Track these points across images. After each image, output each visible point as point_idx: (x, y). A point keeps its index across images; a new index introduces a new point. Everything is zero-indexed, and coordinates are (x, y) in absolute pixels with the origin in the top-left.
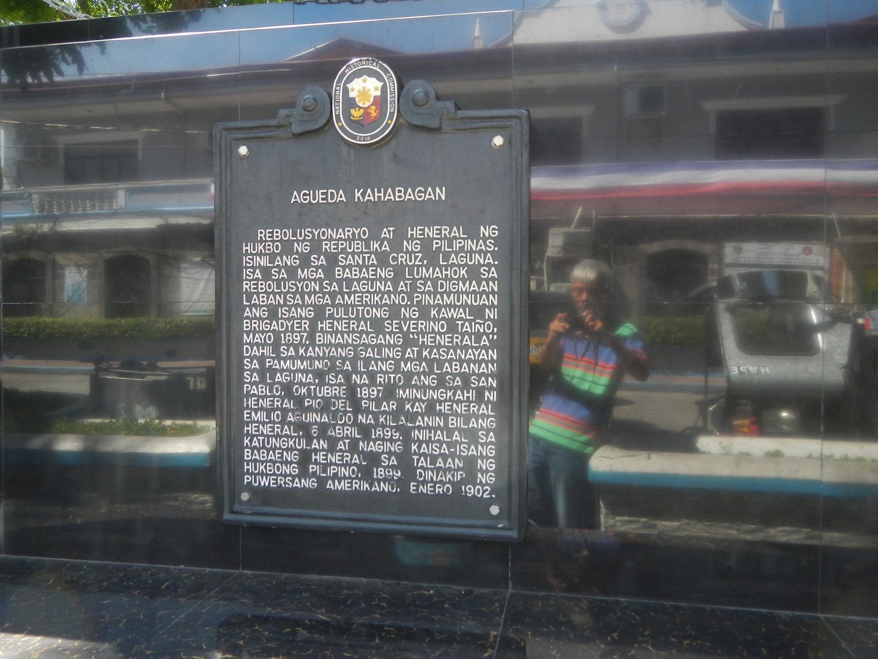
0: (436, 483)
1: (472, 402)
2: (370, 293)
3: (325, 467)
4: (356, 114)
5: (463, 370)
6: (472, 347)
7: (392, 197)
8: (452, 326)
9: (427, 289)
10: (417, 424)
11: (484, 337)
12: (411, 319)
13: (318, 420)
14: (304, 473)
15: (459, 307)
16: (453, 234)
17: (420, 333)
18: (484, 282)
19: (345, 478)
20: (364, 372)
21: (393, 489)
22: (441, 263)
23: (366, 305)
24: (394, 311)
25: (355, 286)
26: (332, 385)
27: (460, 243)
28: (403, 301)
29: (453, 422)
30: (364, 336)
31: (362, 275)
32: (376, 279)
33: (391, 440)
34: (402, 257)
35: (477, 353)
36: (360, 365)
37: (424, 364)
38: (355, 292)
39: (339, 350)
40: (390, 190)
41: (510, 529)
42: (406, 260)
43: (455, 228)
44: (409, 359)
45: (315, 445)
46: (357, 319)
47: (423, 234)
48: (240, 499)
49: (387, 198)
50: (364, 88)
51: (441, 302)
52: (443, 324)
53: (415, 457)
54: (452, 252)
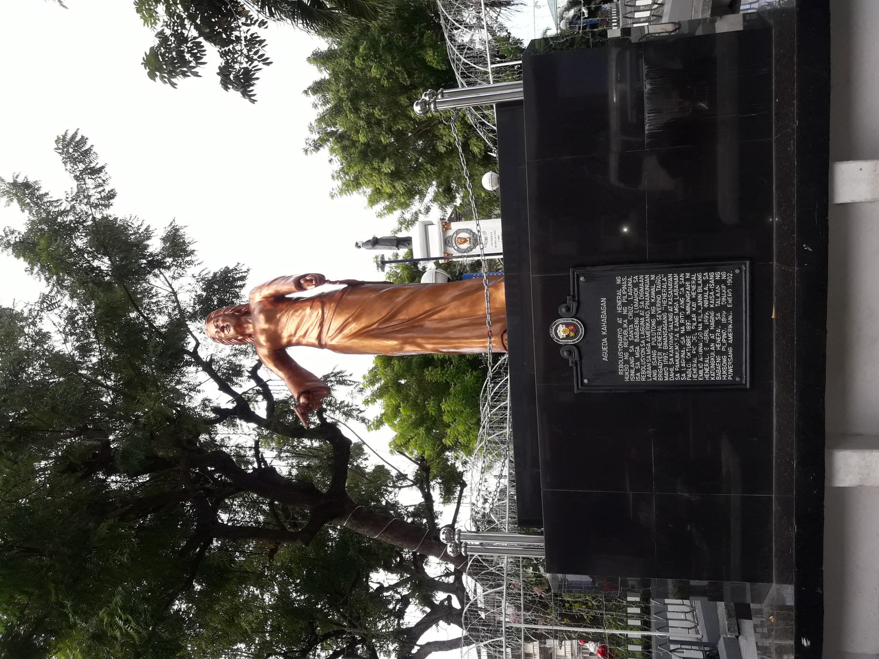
3: (723, 344)
4: (572, 334)
33: (709, 316)
41: (745, 264)
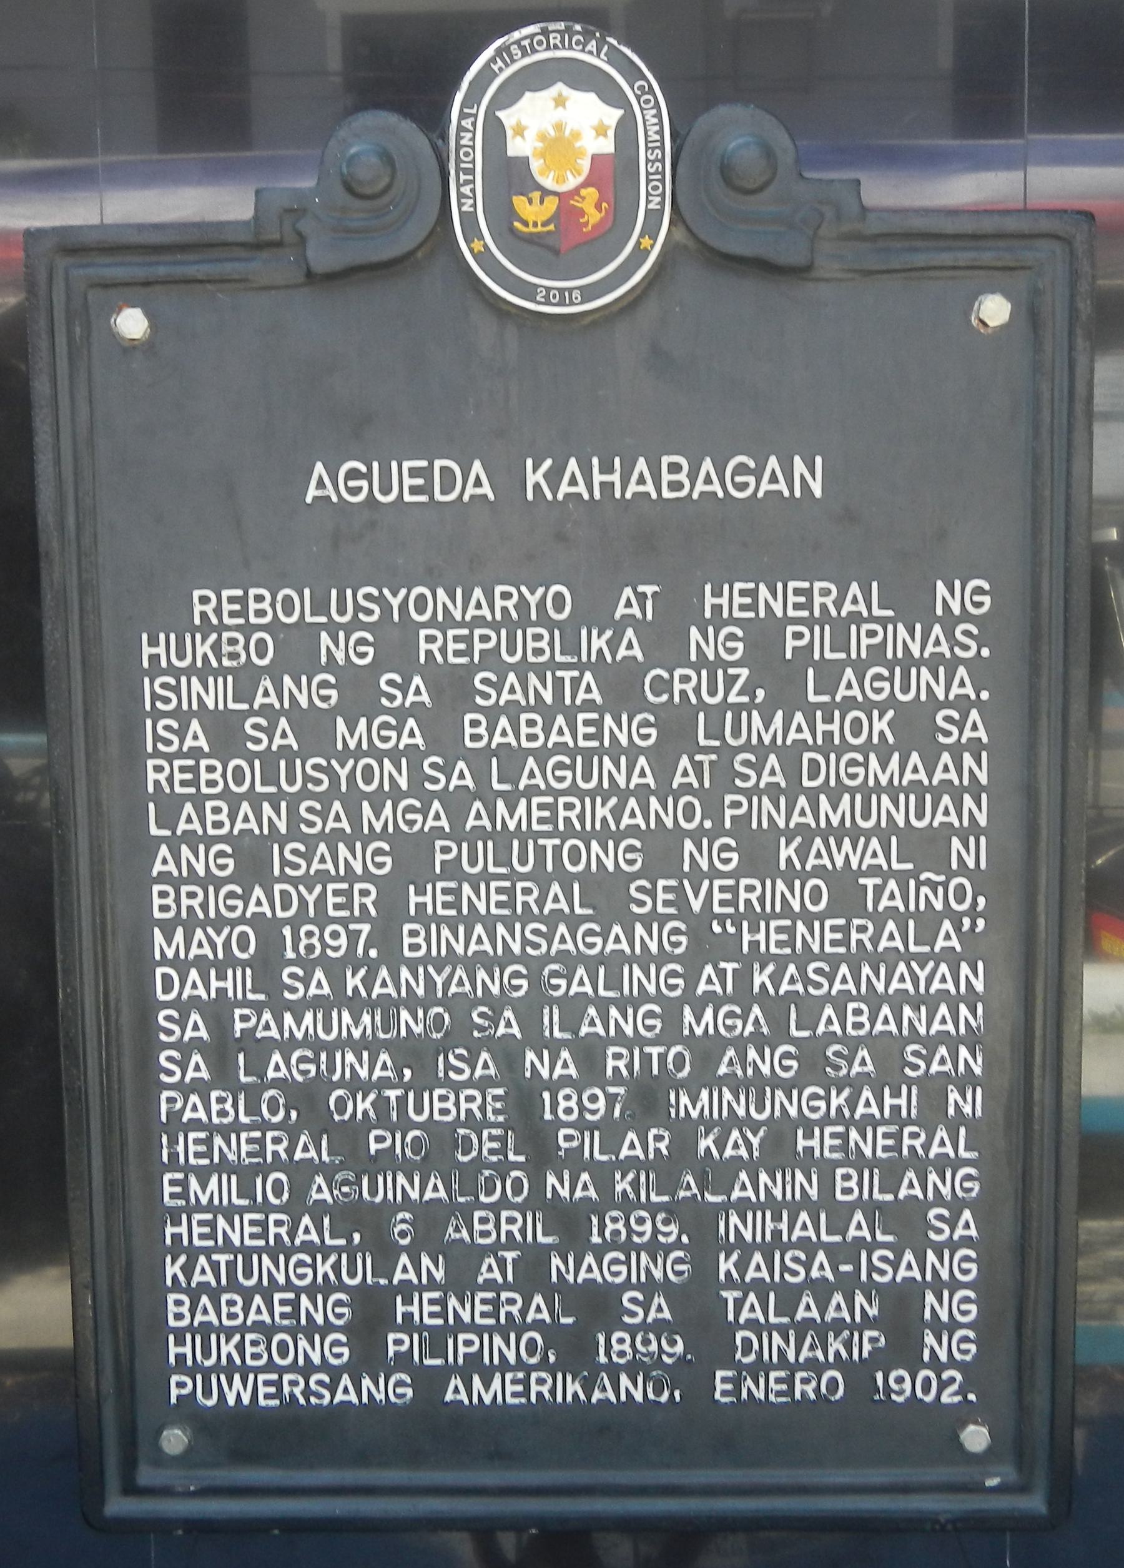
0: (793, 1368)
1: (910, 1122)
2: (581, 794)
3: (436, 1340)
4: (533, 213)
5: (879, 1027)
6: (908, 958)
7: (650, 488)
8: (846, 893)
9: (766, 779)
10: (736, 1194)
11: (947, 925)
12: (714, 874)
13: (414, 1195)
14: (368, 1358)
15: (868, 834)
16: (848, 607)
17: (743, 917)
18: (946, 758)
19: (504, 1366)
20: (564, 1043)
21: (658, 1392)
22: (812, 698)
23: (570, 831)
24: (662, 851)
25: (530, 774)
26: (457, 1087)
27: (872, 634)
28: (689, 818)
29: (848, 1185)
30: (562, 929)
31: (554, 738)
32: (600, 752)
33: (654, 1248)
34: (685, 679)
35: (923, 975)
36: (551, 1020)
37: (756, 1011)
38: (531, 791)
39: (481, 975)
40: (641, 465)
41: (1023, 1489)
42: (697, 690)
43: (854, 589)
44: (710, 996)
45: (403, 1271)
46: (541, 878)
47: (754, 607)
48: (159, 1449)
49: (633, 488)
50: (559, 127)
51: (810, 820)
52: (816, 890)
53: (730, 1296)
54: (848, 662)
